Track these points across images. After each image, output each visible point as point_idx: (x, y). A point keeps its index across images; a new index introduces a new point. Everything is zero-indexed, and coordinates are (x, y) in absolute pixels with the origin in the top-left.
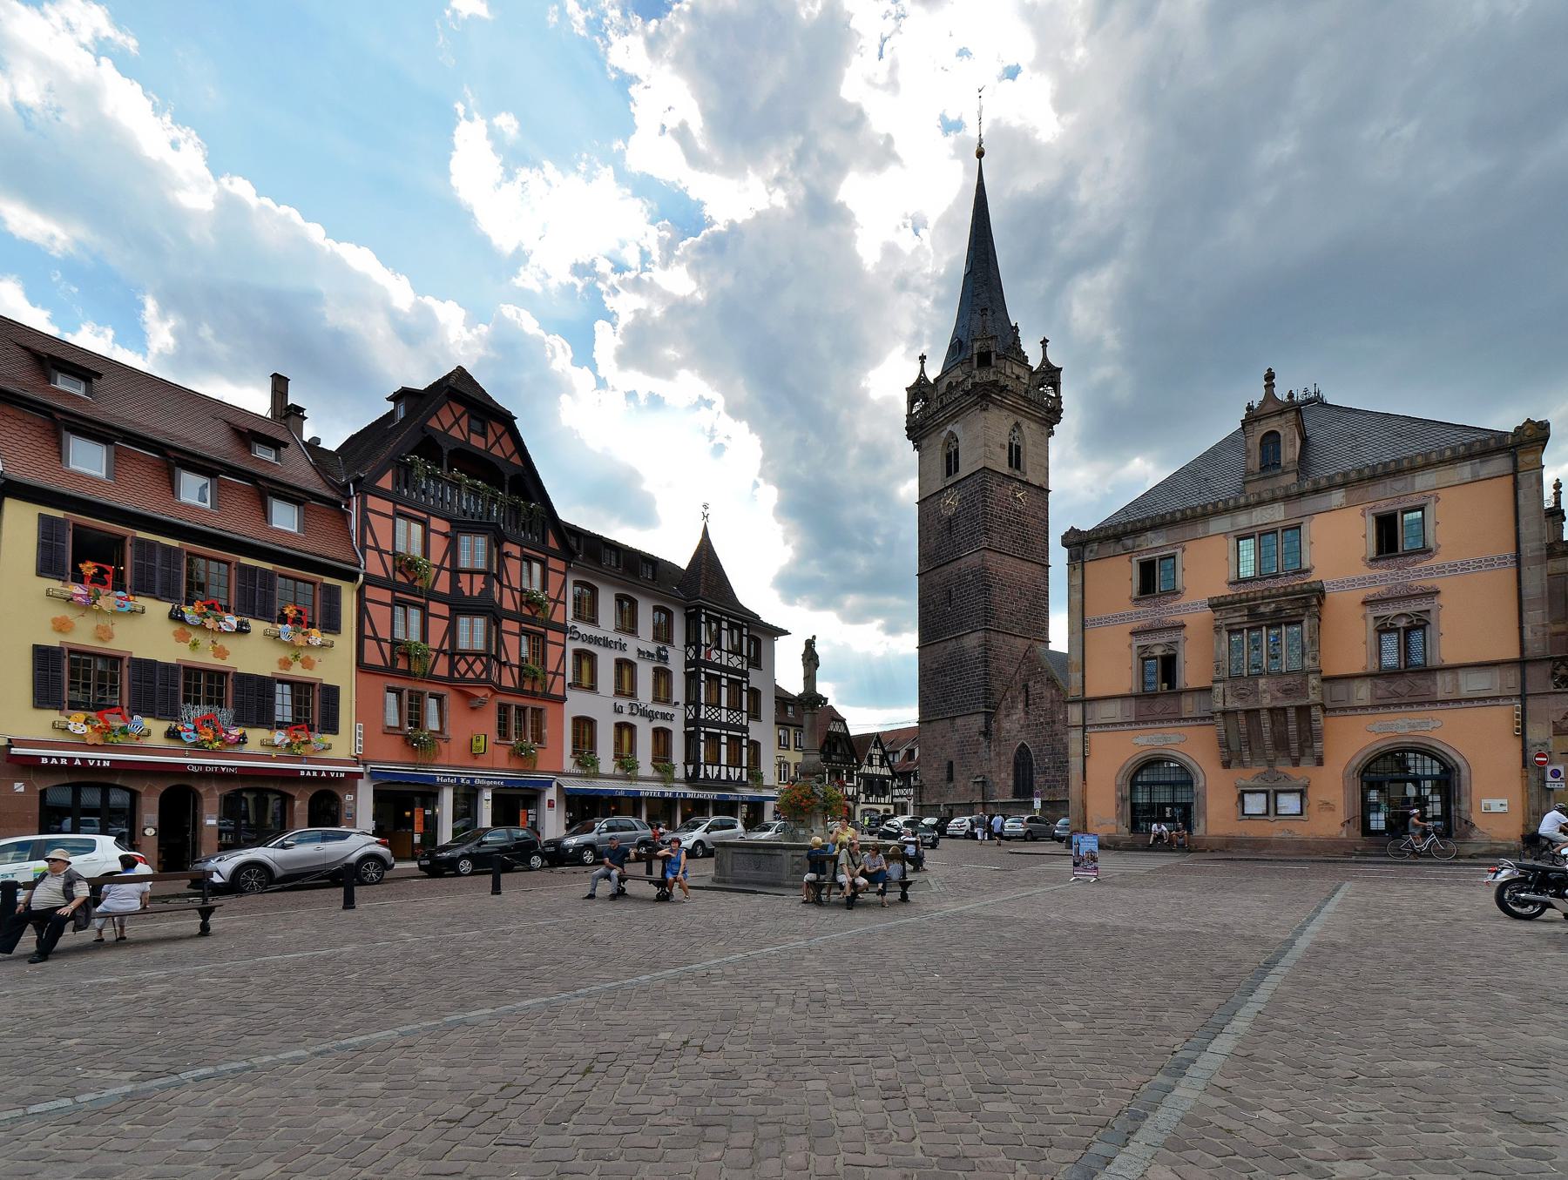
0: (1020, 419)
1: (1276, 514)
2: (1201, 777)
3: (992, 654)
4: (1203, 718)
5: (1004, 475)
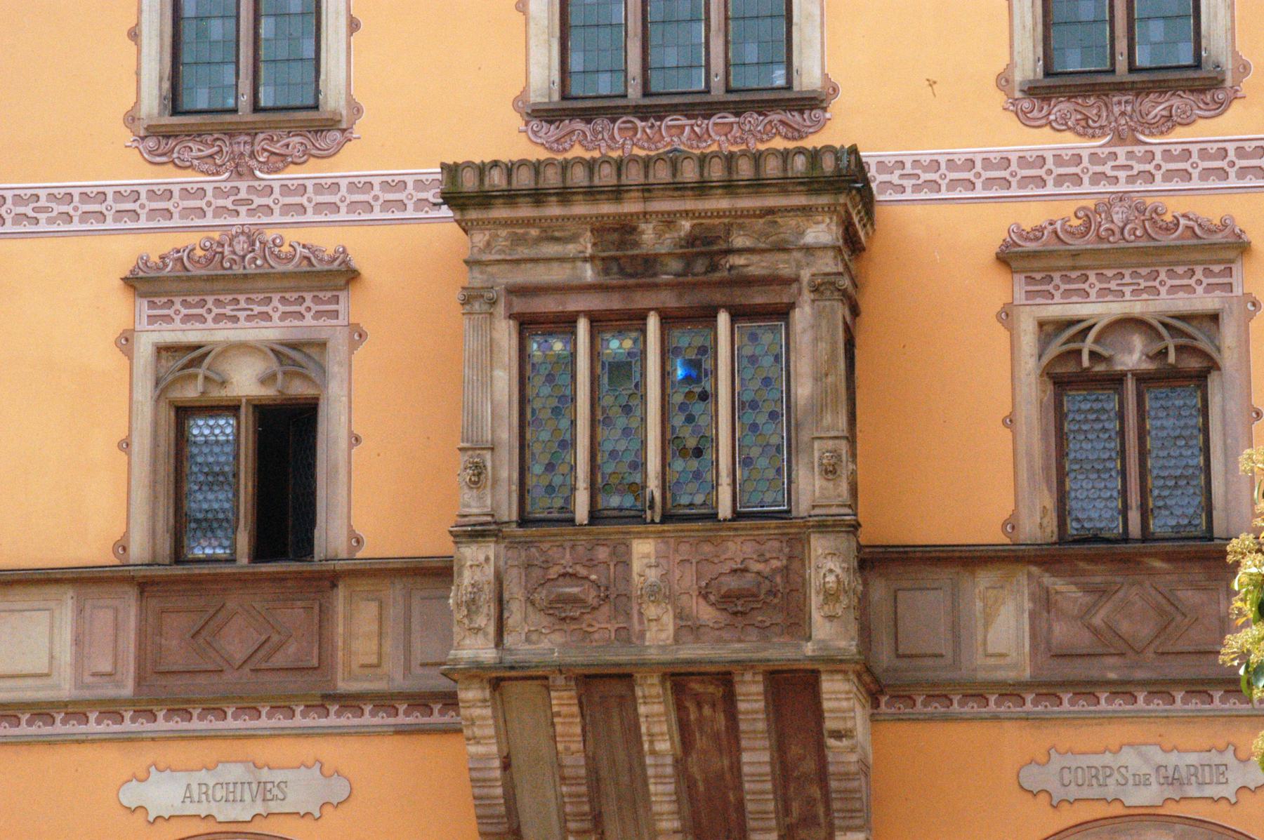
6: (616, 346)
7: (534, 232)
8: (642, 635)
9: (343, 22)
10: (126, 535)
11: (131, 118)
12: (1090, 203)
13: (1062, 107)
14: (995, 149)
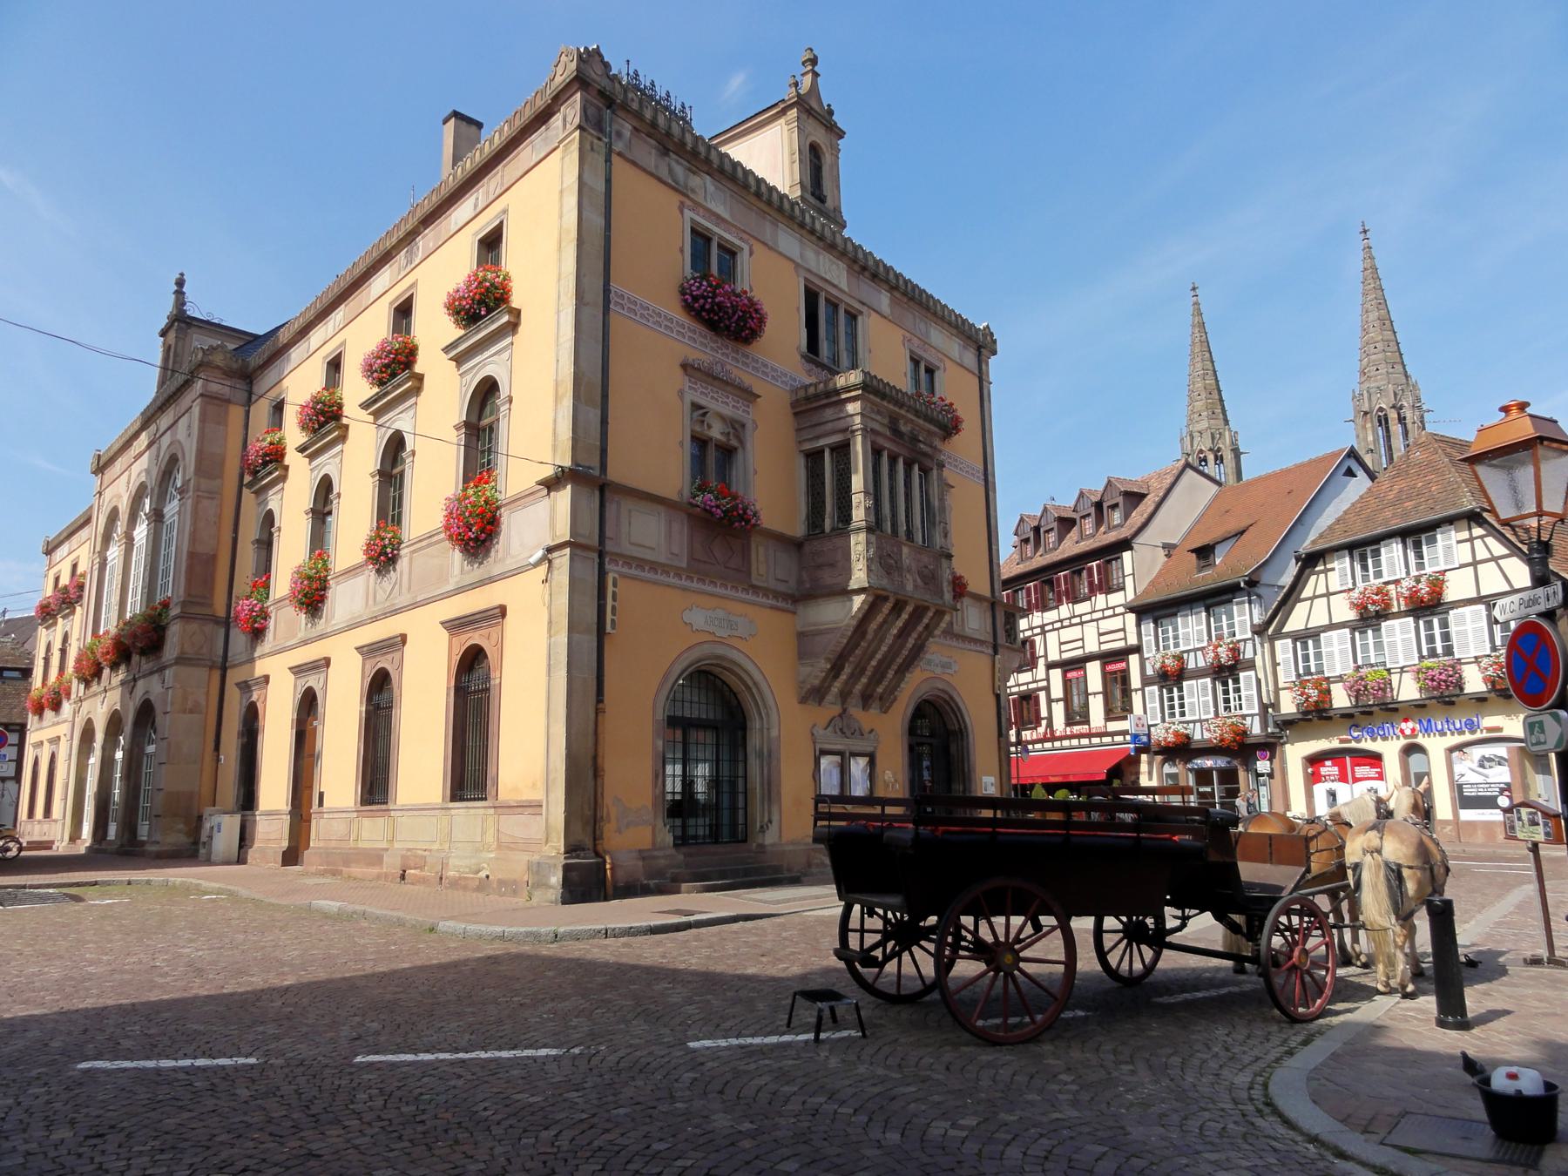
10: (682, 489)
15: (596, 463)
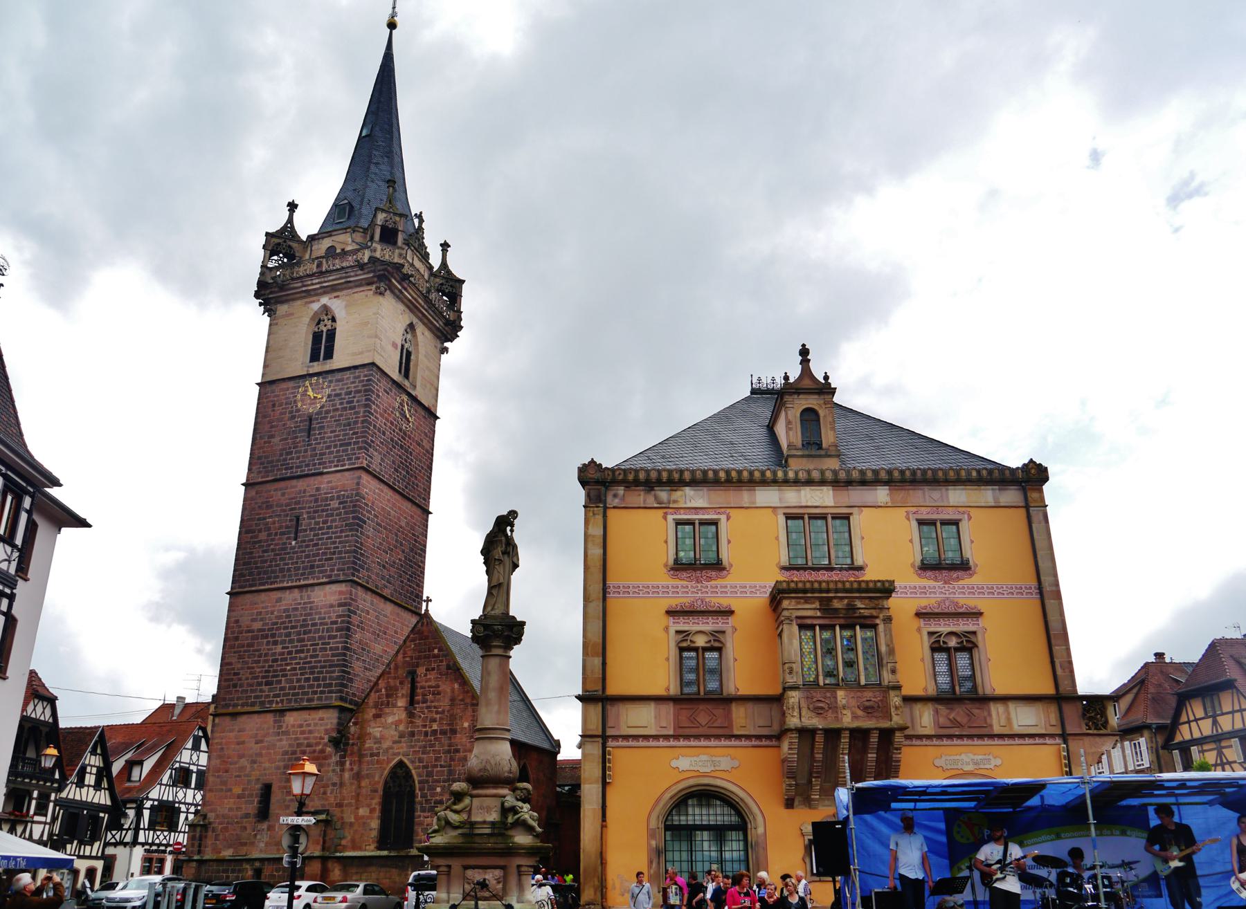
0: (415, 321)
1: (823, 498)
2: (760, 819)
3: (355, 619)
4: (759, 737)
5: (394, 382)
6: (827, 635)
7: (802, 601)
8: (842, 719)
9: (726, 542)
11: (666, 565)
12: (939, 600)
13: (929, 573)
14: (913, 584)
15: (599, 687)
